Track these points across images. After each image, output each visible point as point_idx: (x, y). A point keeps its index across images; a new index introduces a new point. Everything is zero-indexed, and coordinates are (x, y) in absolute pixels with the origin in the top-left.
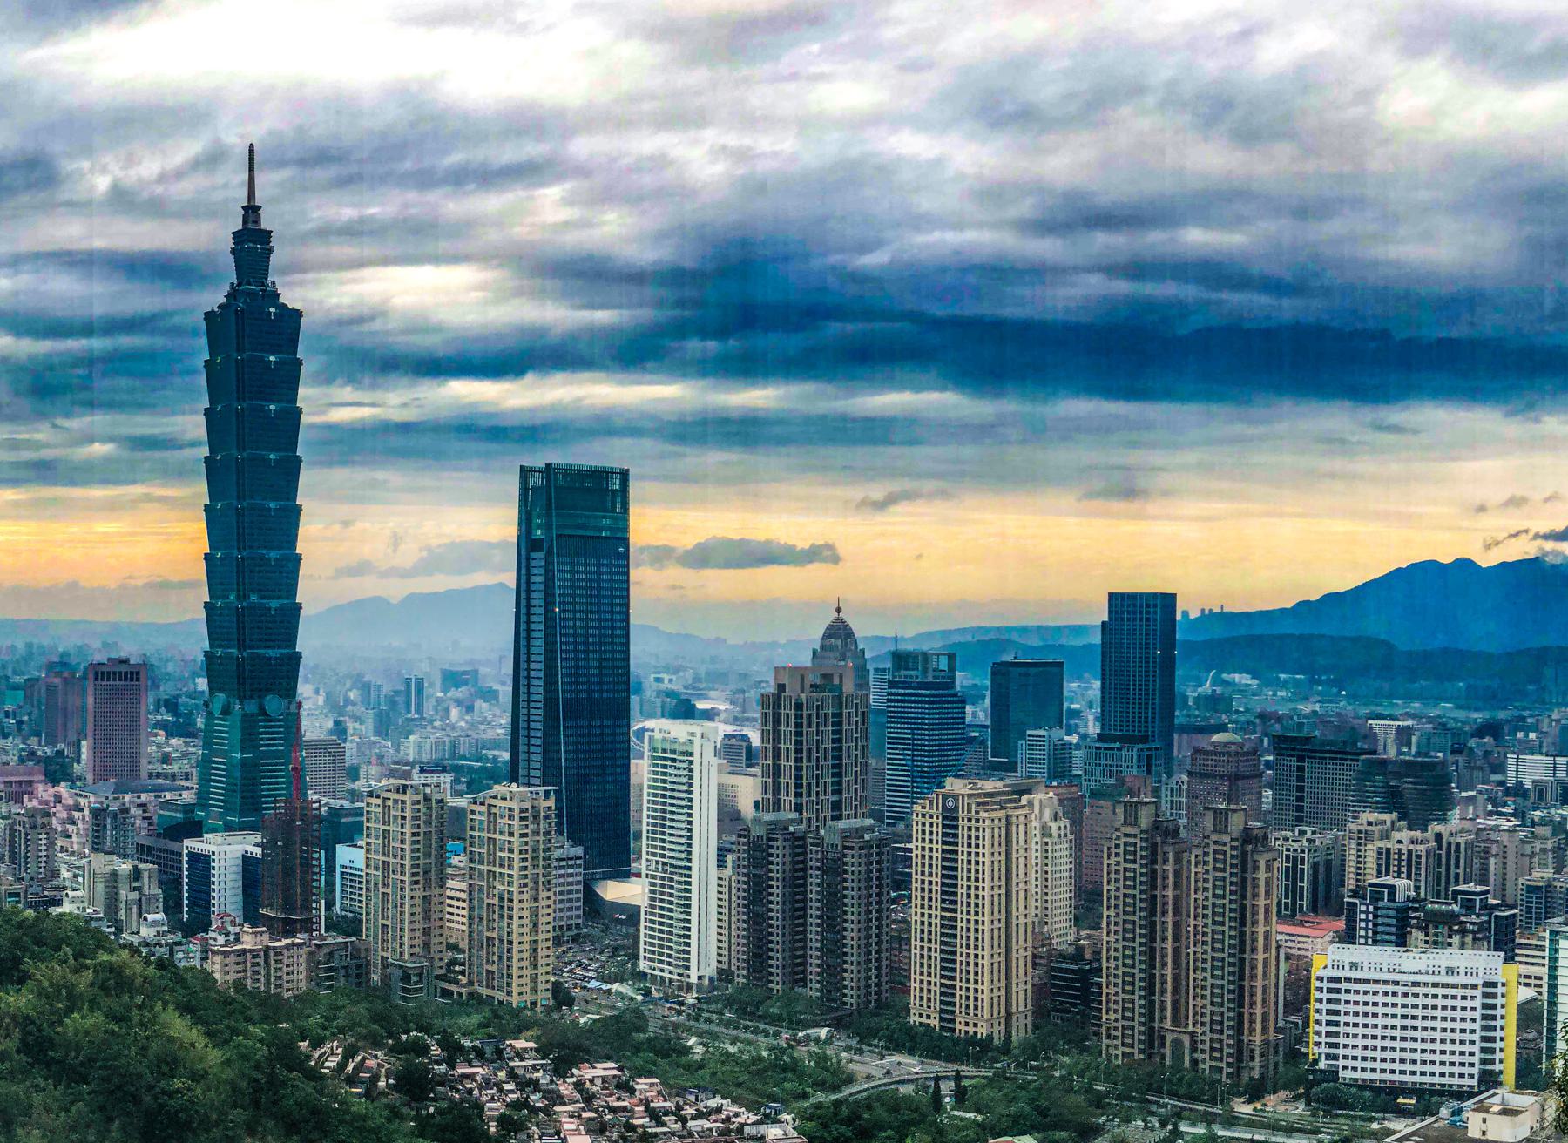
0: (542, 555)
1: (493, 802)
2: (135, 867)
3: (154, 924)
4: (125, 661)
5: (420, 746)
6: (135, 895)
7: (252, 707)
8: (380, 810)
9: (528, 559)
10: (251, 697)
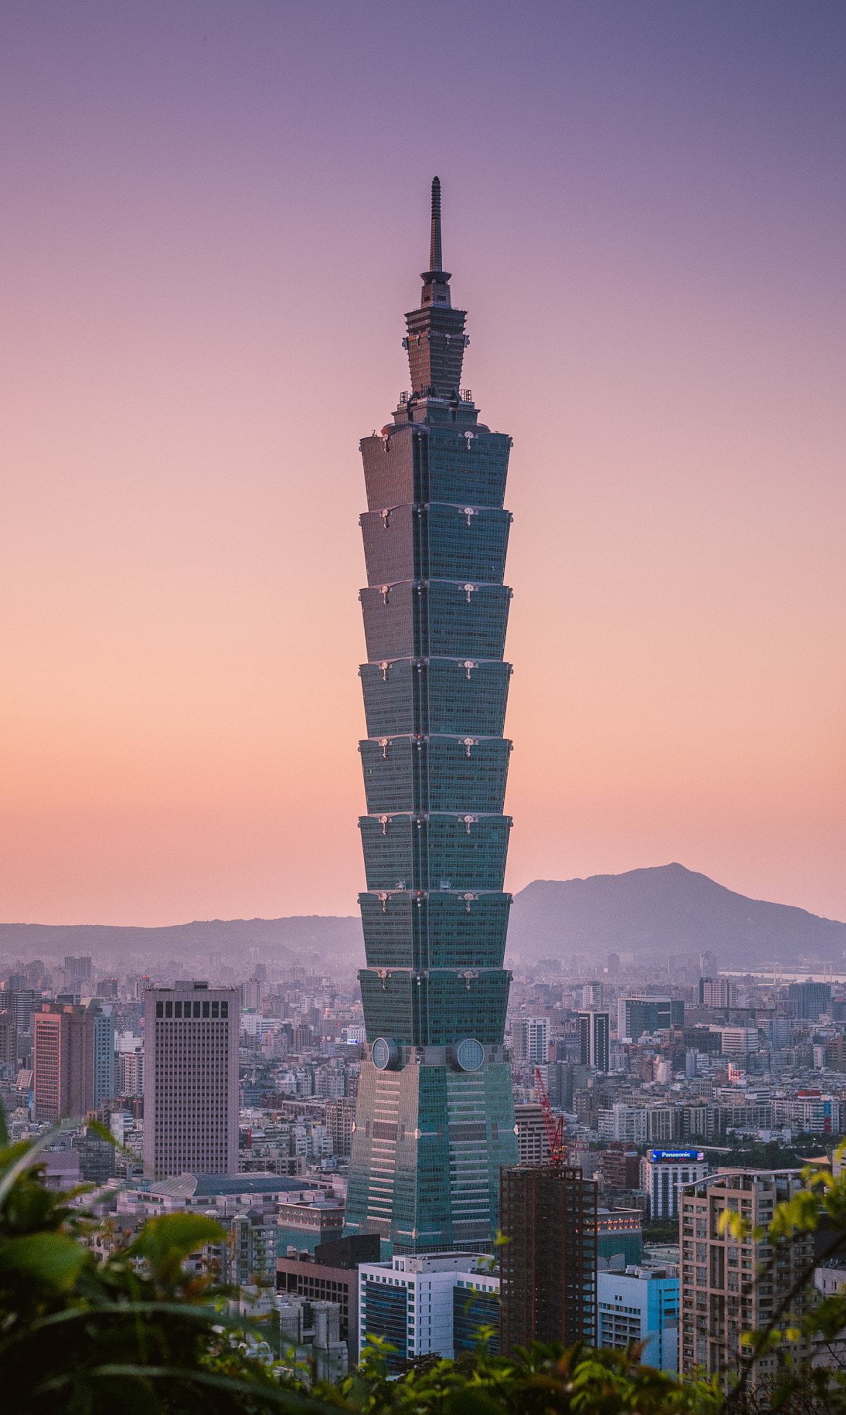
4: (201, 986)
5: (629, 1119)
7: (435, 1055)
10: (436, 1042)
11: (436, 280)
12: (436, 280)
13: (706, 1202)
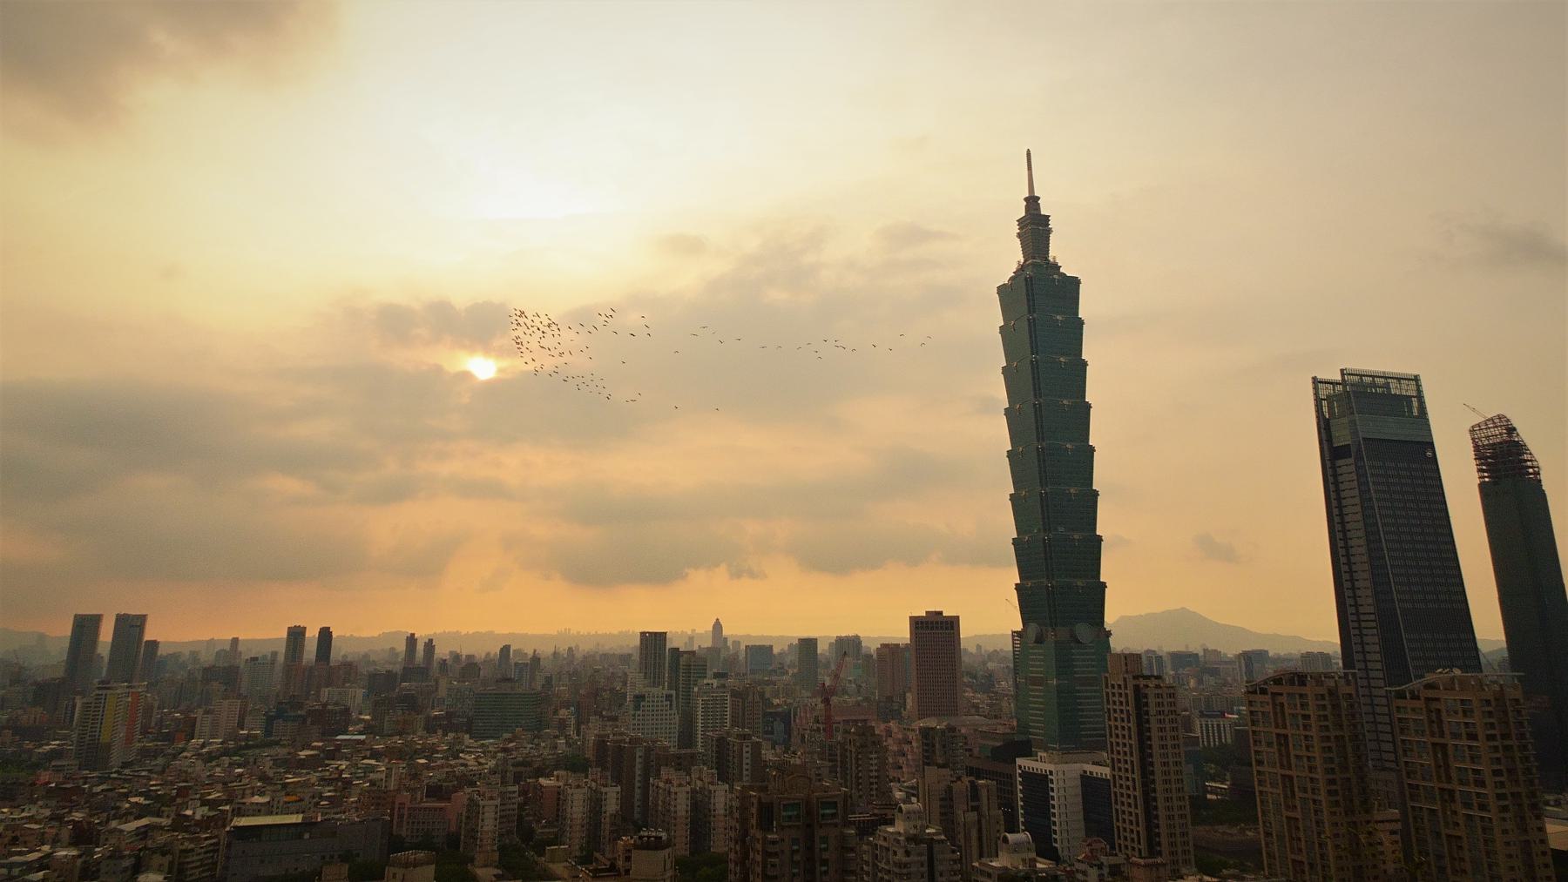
0: (1351, 460)
1: (1431, 693)
2: (972, 782)
3: (1017, 848)
6: (973, 816)
8: (1269, 708)
9: (1334, 467)
11: (1032, 202)
12: (1032, 202)
13: (1268, 698)
